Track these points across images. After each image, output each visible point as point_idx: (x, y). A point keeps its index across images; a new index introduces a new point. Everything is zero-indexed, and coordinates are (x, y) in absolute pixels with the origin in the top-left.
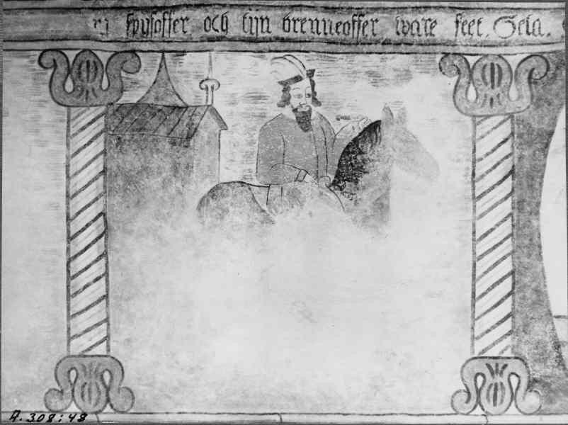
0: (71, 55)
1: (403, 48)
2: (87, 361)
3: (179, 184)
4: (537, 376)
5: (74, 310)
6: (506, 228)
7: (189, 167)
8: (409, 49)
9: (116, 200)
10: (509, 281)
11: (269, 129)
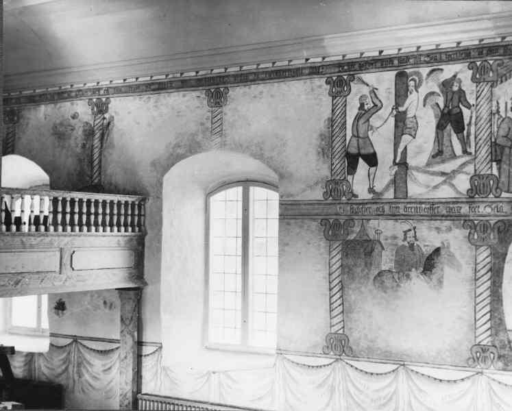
0: (331, 221)
1: (449, 218)
2: (337, 335)
3: (367, 270)
4: (502, 354)
5: (333, 316)
6: (488, 293)
7: (371, 264)
8: (452, 218)
9: (346, 276)
10: (489, 314)
11: (399, 251)
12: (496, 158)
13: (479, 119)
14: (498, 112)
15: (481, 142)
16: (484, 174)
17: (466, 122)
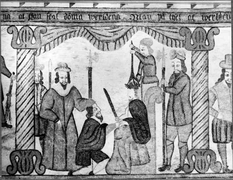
12: (39, 132)
13: (20, 88)
14: (41, 83)
15: (23, 114)
16: (27, 150)
17: (6, 91)
